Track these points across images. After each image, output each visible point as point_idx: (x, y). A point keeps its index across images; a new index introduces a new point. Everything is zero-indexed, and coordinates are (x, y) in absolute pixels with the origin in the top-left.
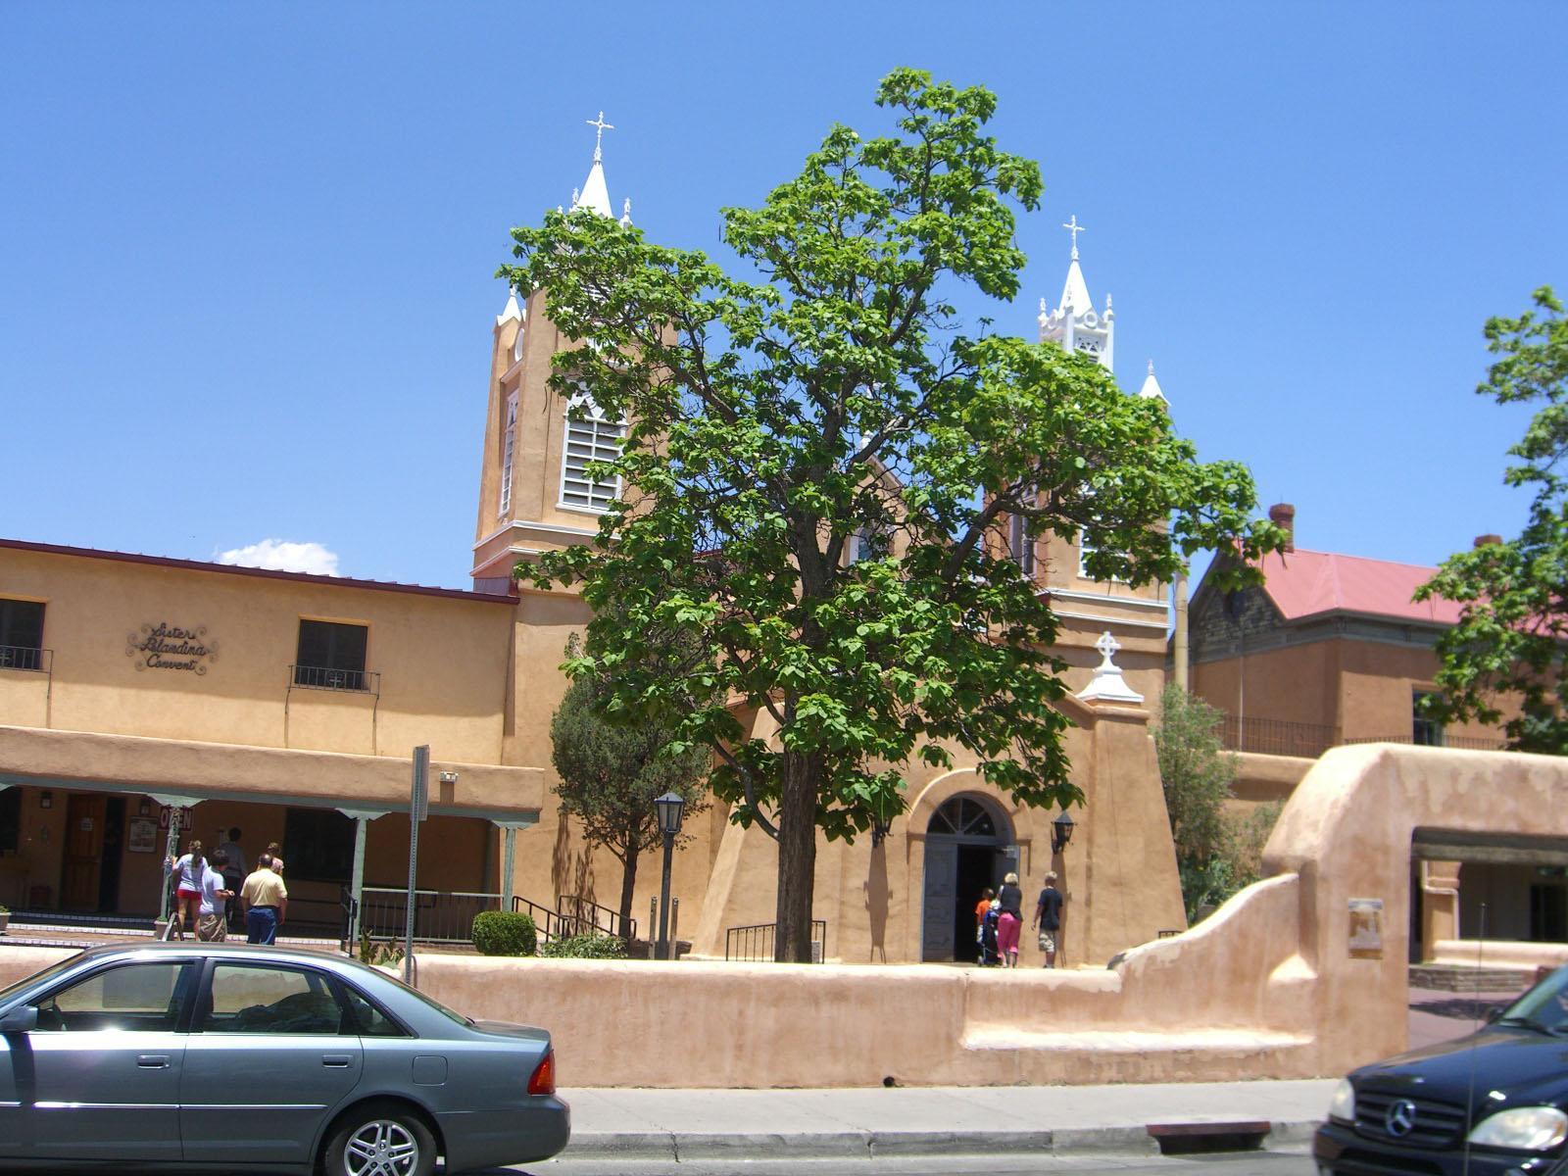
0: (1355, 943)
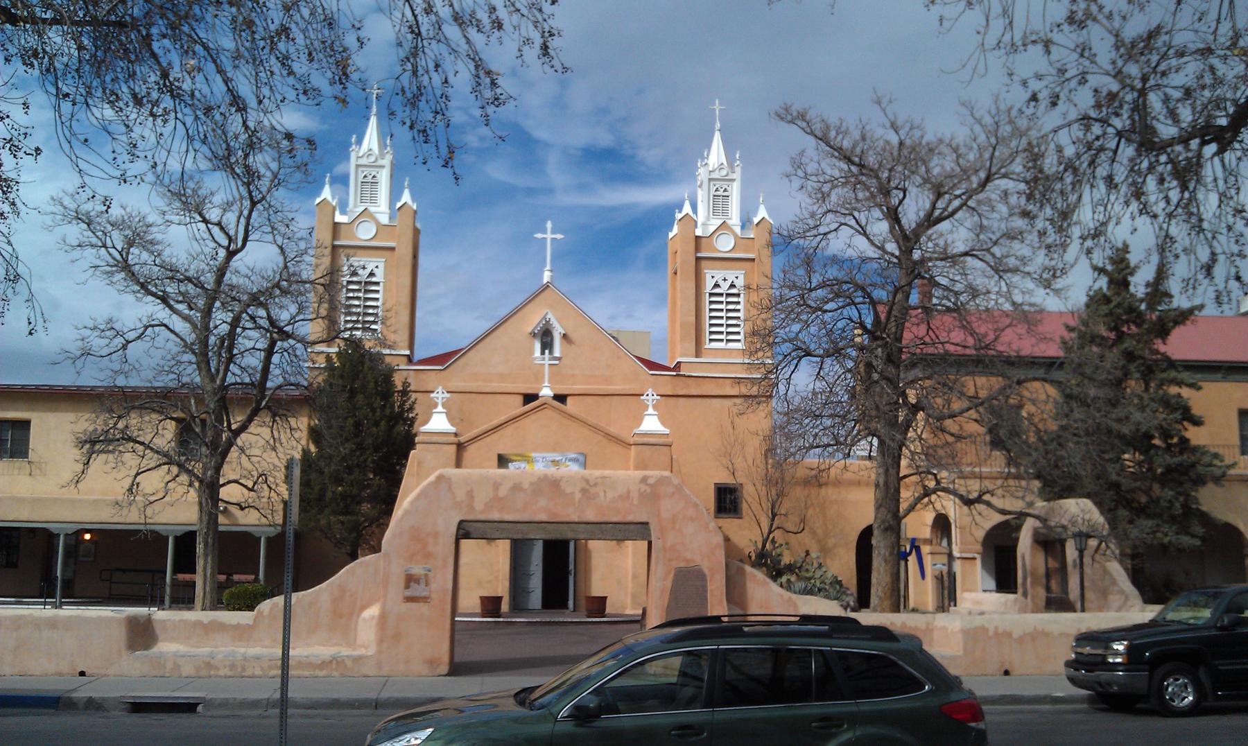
0: (409, 593)
